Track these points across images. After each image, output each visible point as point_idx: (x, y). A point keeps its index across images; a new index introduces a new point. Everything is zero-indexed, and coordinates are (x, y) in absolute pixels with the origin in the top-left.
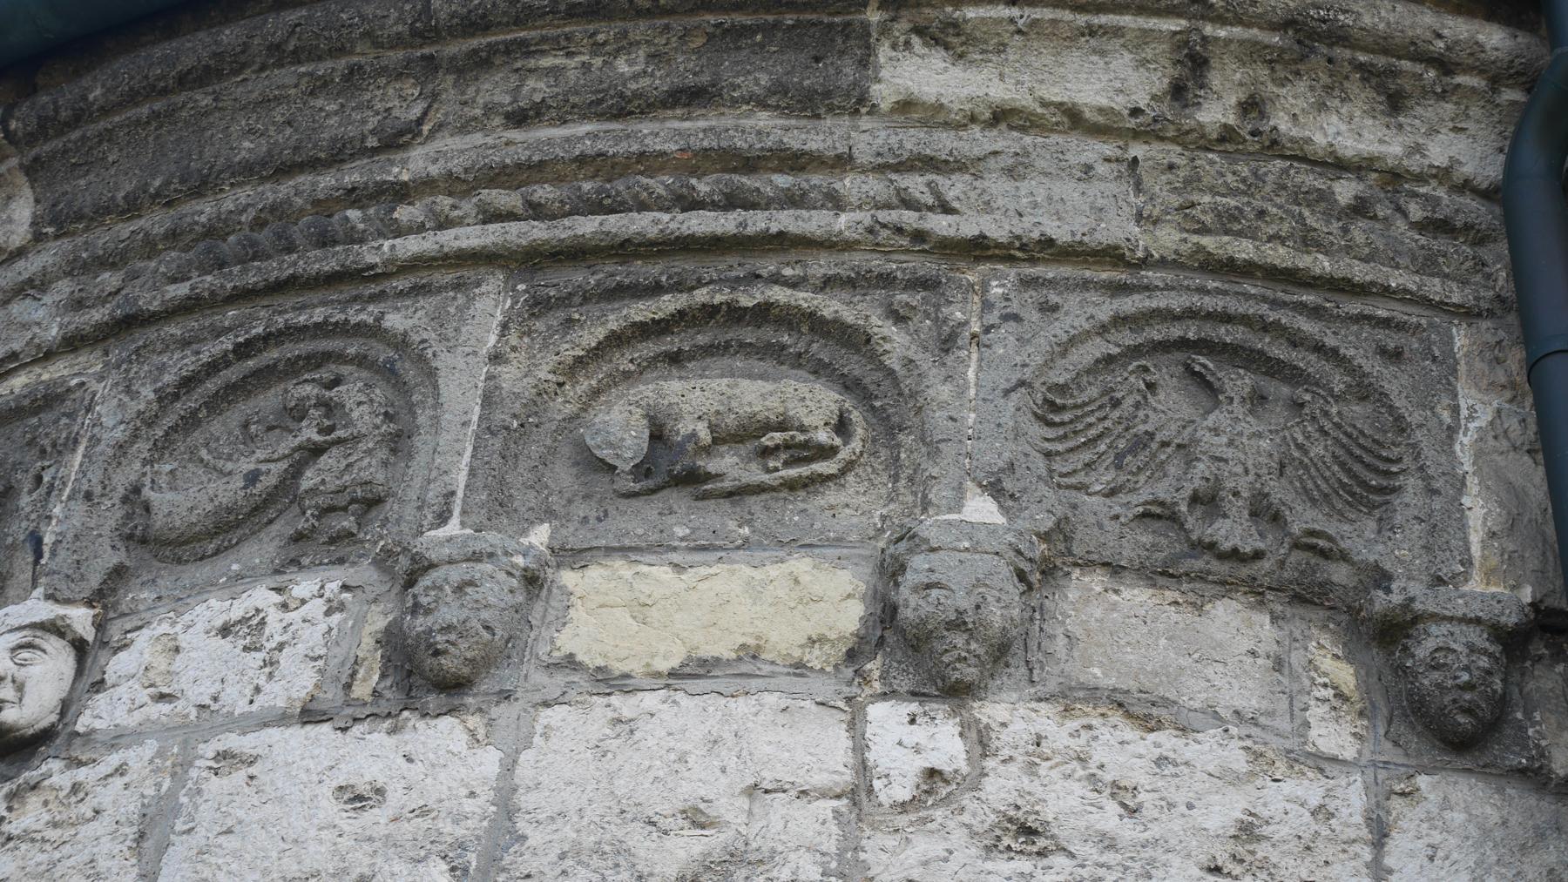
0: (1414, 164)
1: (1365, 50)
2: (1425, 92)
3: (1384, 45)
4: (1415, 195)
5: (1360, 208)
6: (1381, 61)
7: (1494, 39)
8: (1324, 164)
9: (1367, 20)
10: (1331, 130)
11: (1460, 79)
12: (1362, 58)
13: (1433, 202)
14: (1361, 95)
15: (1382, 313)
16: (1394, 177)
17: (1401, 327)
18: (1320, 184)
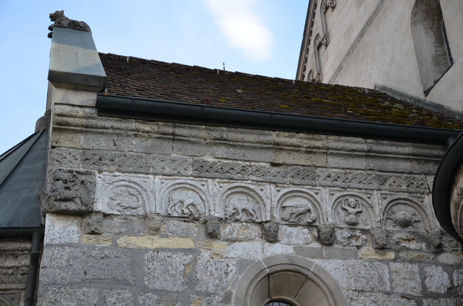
0: (20, 265)
1: (10, 251)
2: (20, 255)
3: (12, 250)
4: (20, 269)
5: (12, 274)
6: (13, 252)
7: (28, 245)
8: (7, 268)
9: (9, 248)
10: (7, 263)
11: (24, 252)
12: (10, 253)
13: (23, 270)
14: (11, 258)
15: (12, 292)
16: (17, 268)
17: (15, 294)
18: (6, 272)
